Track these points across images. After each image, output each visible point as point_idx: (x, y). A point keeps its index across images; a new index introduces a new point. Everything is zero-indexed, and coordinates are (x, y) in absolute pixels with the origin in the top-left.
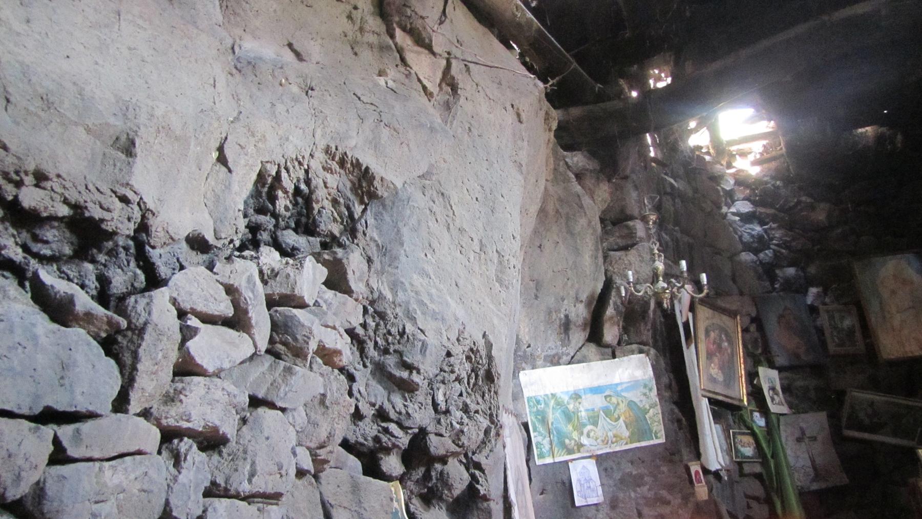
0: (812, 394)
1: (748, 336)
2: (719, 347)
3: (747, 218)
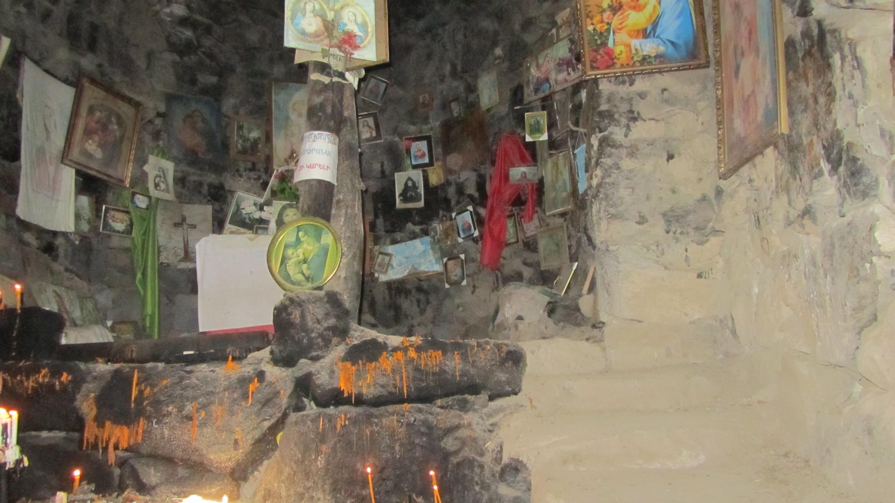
0: (205, 190)
1: (150, 128)
2: (104, 127)
3: (183, 22)
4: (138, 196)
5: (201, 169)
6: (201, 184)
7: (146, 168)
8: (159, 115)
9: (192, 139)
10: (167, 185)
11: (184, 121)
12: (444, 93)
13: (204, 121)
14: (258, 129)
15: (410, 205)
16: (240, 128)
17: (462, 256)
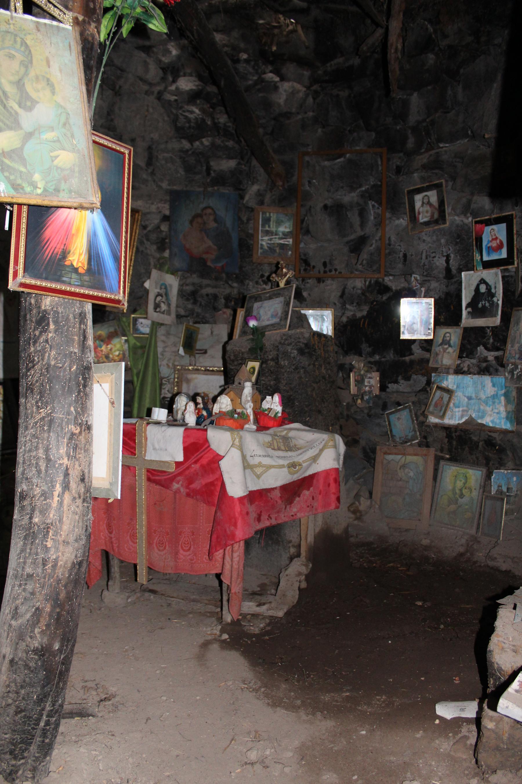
3: (193, 97)
4: (141, 320)
6: (215, 297)
7: (147, 285)
8: (165, 218)
9: (201, 244)
10: (169, 305)
11: (191, 222)
13: (215, 220)
15: (480, 322)
16: (267, 221)
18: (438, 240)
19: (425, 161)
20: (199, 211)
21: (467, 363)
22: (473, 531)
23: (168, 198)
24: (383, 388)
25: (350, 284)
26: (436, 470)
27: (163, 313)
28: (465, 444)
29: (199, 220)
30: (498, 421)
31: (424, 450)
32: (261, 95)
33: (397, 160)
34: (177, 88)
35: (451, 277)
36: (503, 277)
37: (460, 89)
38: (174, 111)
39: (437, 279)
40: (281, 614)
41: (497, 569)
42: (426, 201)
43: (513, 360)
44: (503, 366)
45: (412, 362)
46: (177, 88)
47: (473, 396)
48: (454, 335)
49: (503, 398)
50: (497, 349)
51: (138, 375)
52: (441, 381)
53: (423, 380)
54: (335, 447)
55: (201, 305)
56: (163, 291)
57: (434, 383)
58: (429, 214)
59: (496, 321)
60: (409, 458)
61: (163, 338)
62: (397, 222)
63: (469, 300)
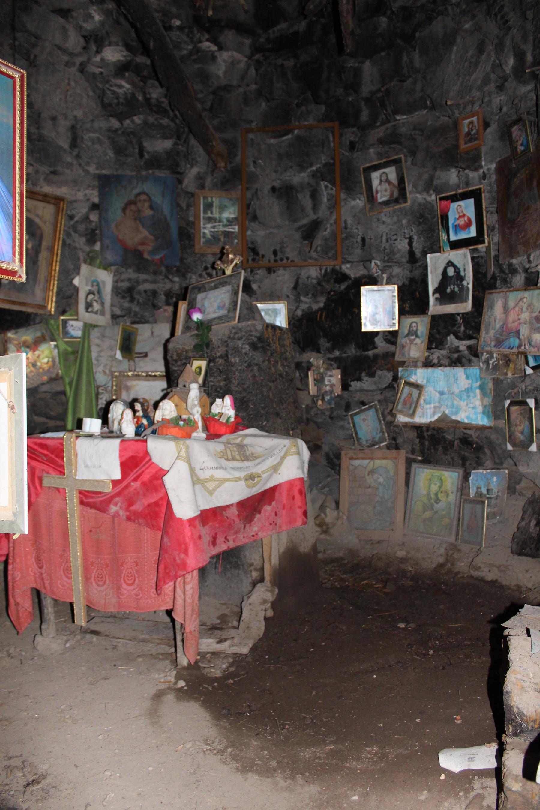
3: (122, 69)
4: (71, 323)
5: (155, 273)
6: (155, 293)
8: (95, 207)
9: (135, 235)
10: (103, 304)
11: (124, 210)
12: (505, 109)
13: (151, 207)
14: (233, 205)
15: (450, 309)
16: (209, 206)
17: (531, 402)
18: (399, 221)
19: (381, 134)
20: (132, 198)
21: (437, 354)
22: (452, 539)
23: (96, 183)
24: (345, 386)
25: (304, 273)
26: (408, 474)
27: (96, 313)
28: (439, 444)
29: (133, 207)
30: (474, 417)
31: (394, 452)
32: (197, 66)
33: (350, 135)
34: (102, 59)
35: (415, 260)
36: (473, 258)
37: (416, 55)
38: (100, 85)
39: (399, 264)
40: (245, 650)
41: (482, 580)
42: (384, 178)
43: (488, 349)
44: (476, 355)
45: (376, 356)
46: (102, 59)
47: (446, 390)
48: (421, 324)
49: (478, 391)
50: (470, 338)
51: (70, 384)
52: (409, 375)
53: (389, 376)
54: (298, 453)
55: (138, 302)
56: (95, 289)
57: (401, 379)
58: (388, 193)
59: (467, 306)
60: (378, 462)
61: (97, 341)
62: (353, 203)
63: (436, 285)
